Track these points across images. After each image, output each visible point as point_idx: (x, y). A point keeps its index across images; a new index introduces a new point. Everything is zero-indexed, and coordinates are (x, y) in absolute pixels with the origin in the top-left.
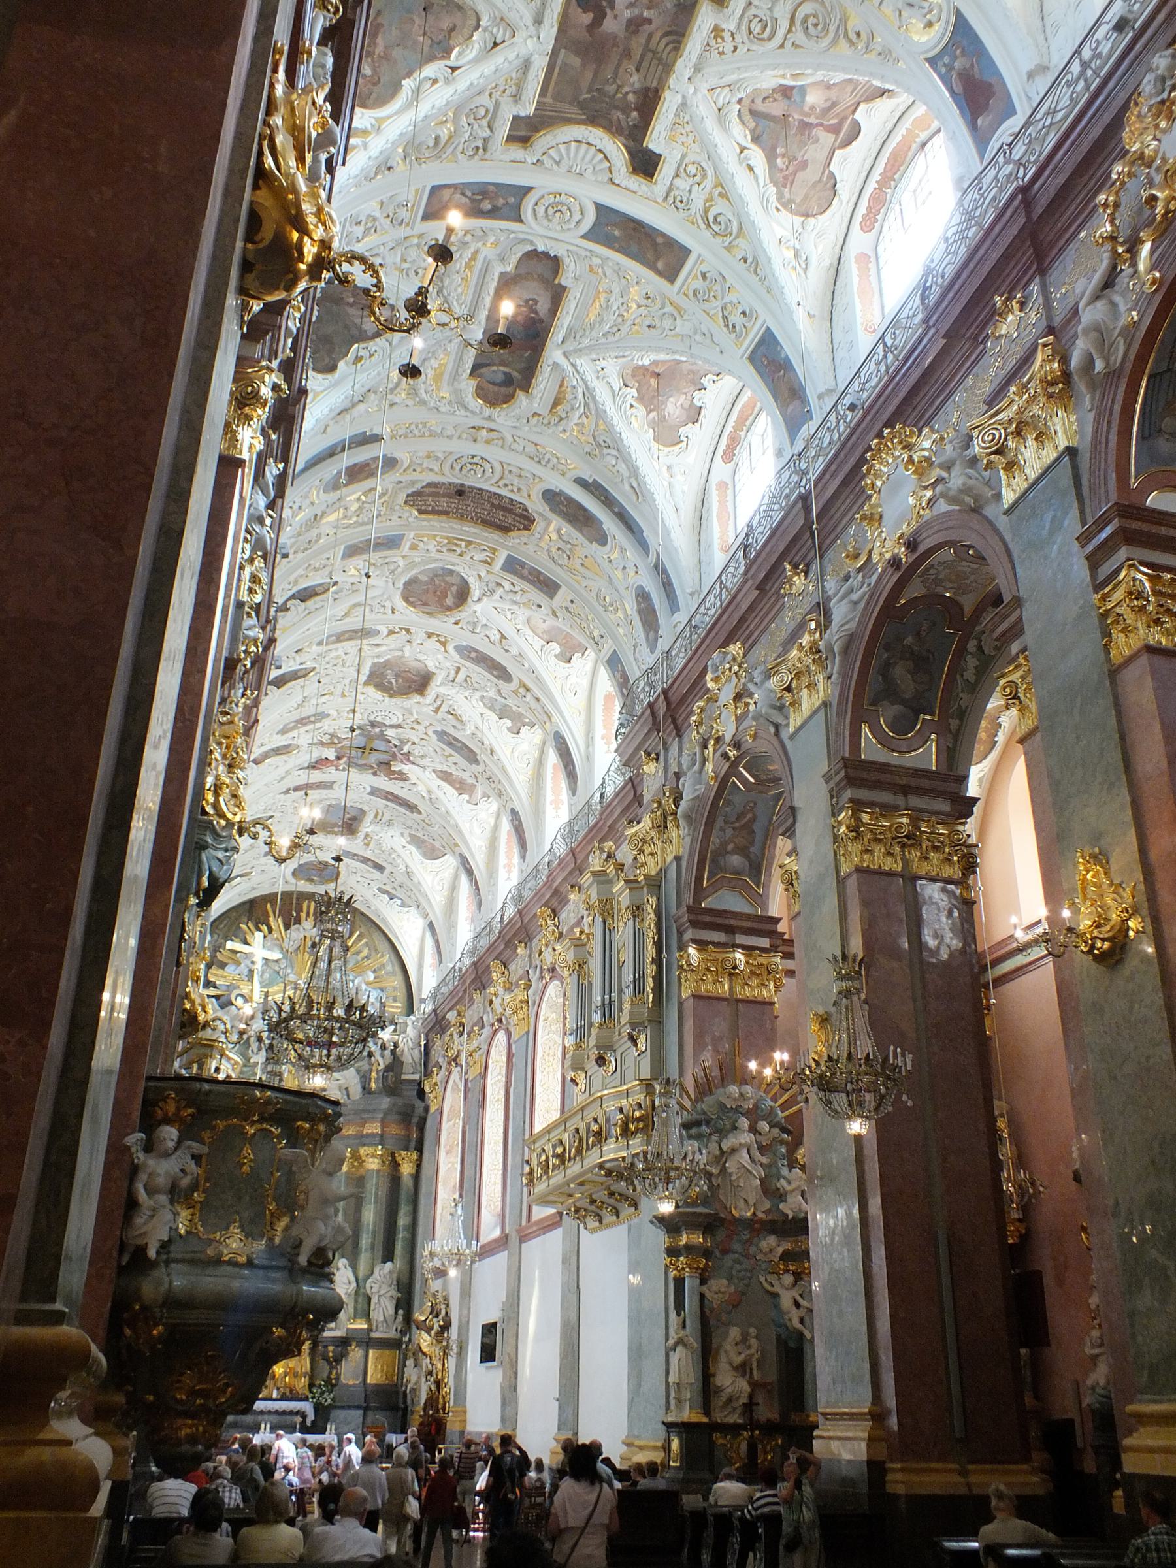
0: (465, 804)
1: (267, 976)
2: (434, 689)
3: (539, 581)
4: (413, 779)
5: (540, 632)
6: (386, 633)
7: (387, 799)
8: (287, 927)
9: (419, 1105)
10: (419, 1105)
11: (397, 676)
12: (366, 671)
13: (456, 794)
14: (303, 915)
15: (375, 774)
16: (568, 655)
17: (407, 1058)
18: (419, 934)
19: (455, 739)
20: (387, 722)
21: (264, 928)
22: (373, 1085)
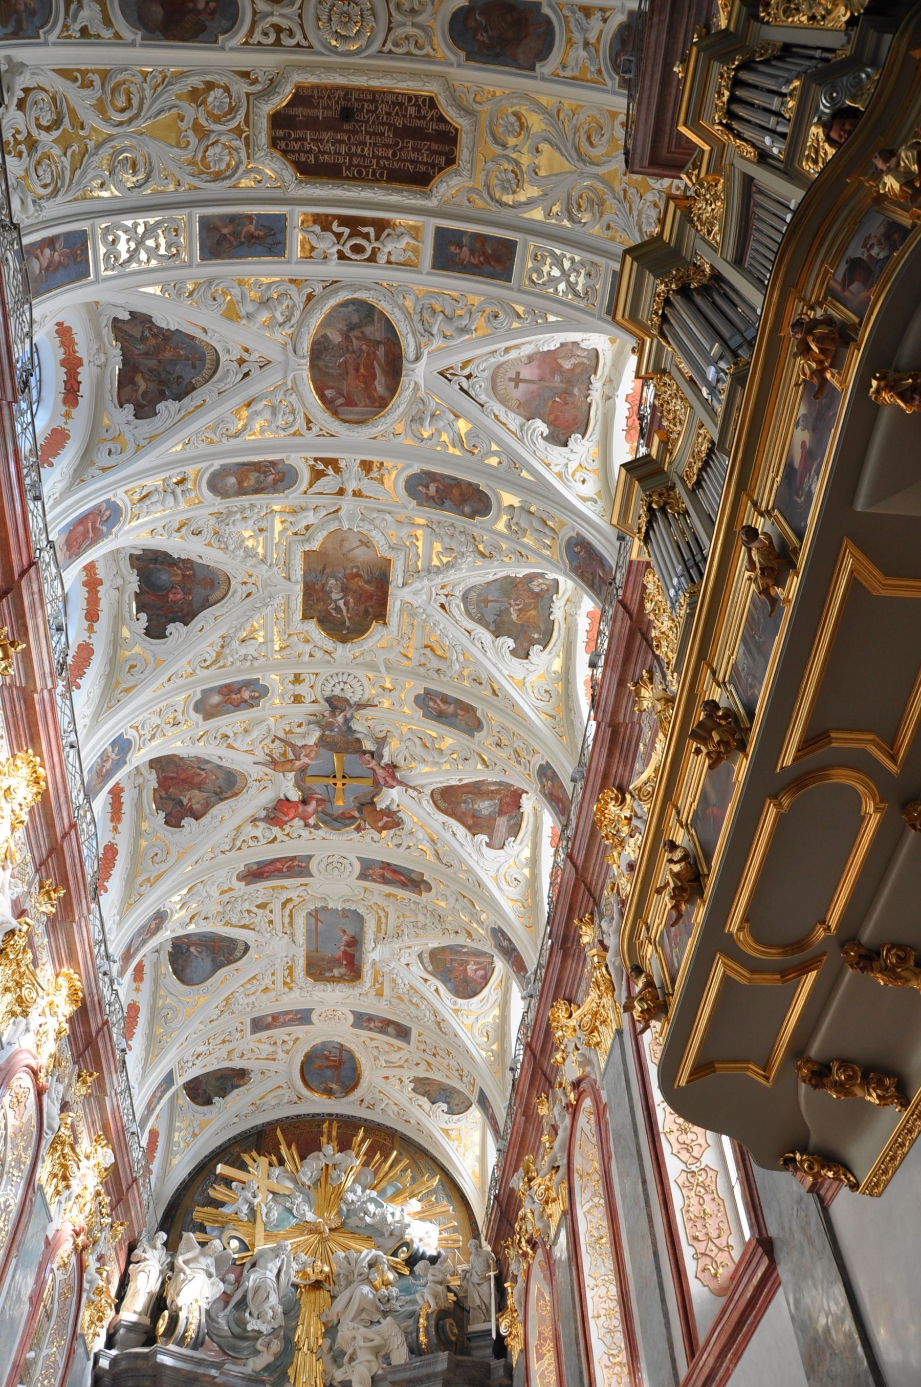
0: (485, 849)
1: (275, 1214)
2: (397, 598)
3: (488, 258)
4: (408, 825)
5: (514, 403)
6: (305, 475)
7: (385, 881)
8: (303, 1158)
9: (497, 1364)
10: (497, 1364)
11: (344, 590)
12: (298, 573)
13: (470, 836)
14: (324, 1139)
15: (358, 829)
16: (563, 438)
17: (474, 1300)
18: (477, 1151)
19: (445, 699)
20: (348, 695)
21: (274, 1158)
22: (423, 1339)
